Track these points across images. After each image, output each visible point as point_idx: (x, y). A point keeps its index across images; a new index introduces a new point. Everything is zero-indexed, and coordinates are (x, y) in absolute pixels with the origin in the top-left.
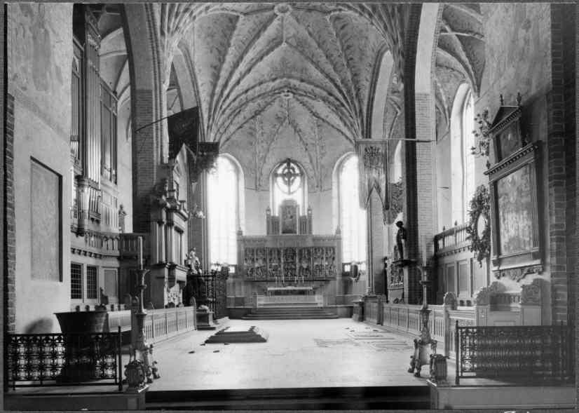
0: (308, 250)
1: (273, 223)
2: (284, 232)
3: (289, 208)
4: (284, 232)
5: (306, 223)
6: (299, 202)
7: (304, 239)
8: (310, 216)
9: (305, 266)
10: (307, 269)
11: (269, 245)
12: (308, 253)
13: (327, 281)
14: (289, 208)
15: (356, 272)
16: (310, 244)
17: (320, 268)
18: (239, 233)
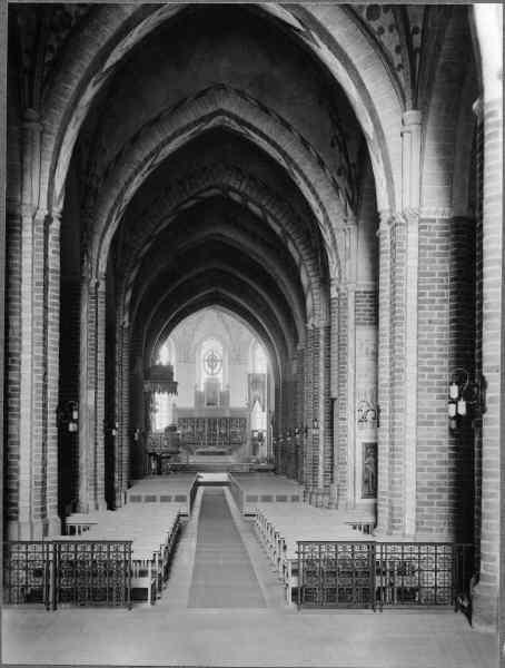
0: (226, 419)
1: (199, 397)
2: (208, 404)
3: (211, 385)
4: (208, 404)
5: (225, 397)
6: (221, 381)
7: (223, 410)
8: (228, 392)
9: (222, 431)
10: (226, 435)
11: (196, 415)
12: (228, 422)
13: (240, 444)
14: (211, 385)
15: (261, 438)
16: (228, 415)
17: (235, 434)
18: (174, 405)
